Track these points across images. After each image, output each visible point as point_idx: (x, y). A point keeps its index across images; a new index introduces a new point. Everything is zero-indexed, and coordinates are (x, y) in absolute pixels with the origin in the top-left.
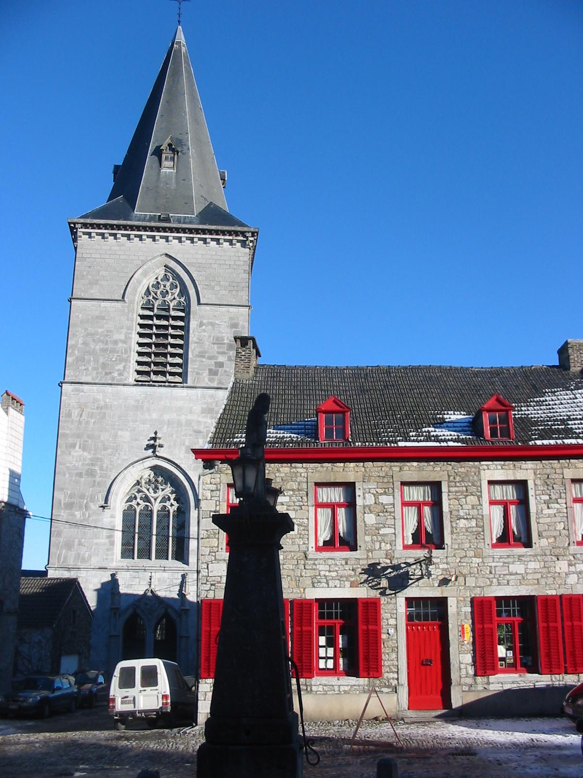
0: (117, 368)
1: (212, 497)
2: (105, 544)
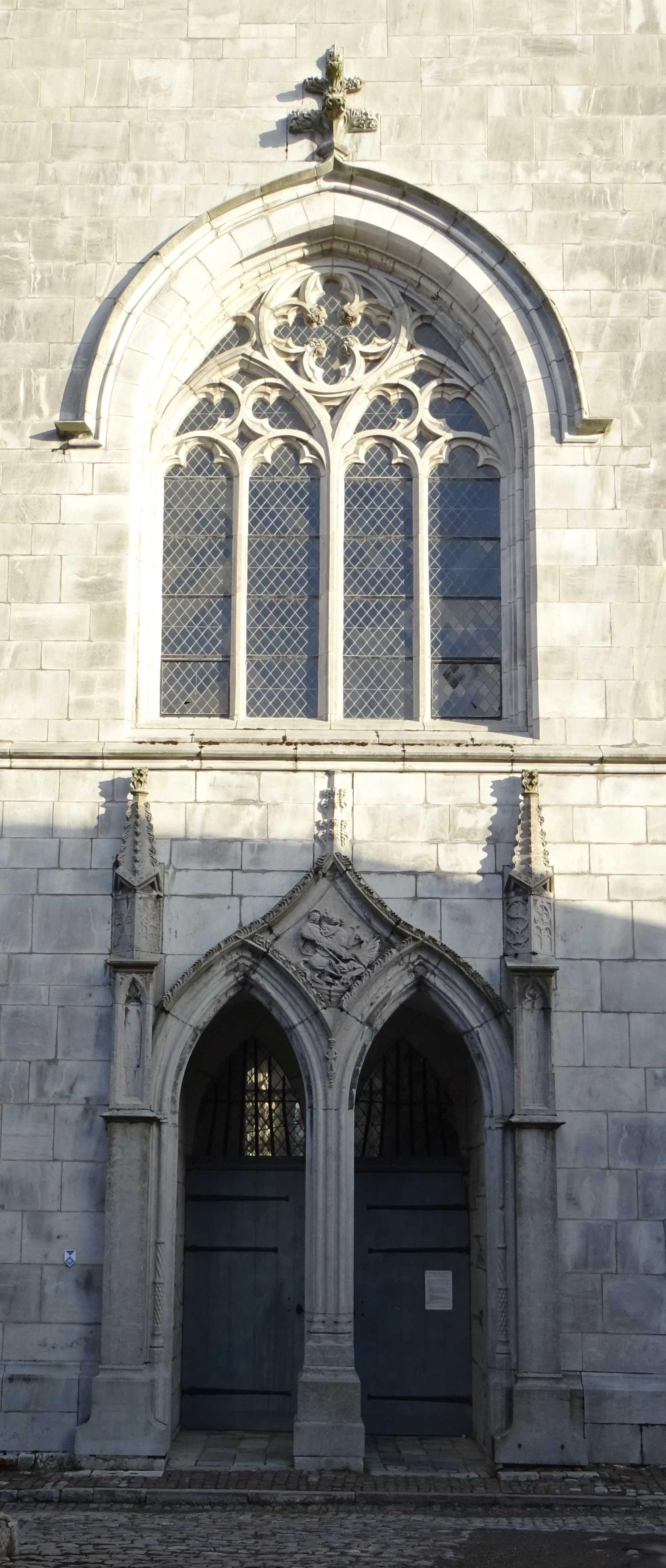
2: (70, 630)
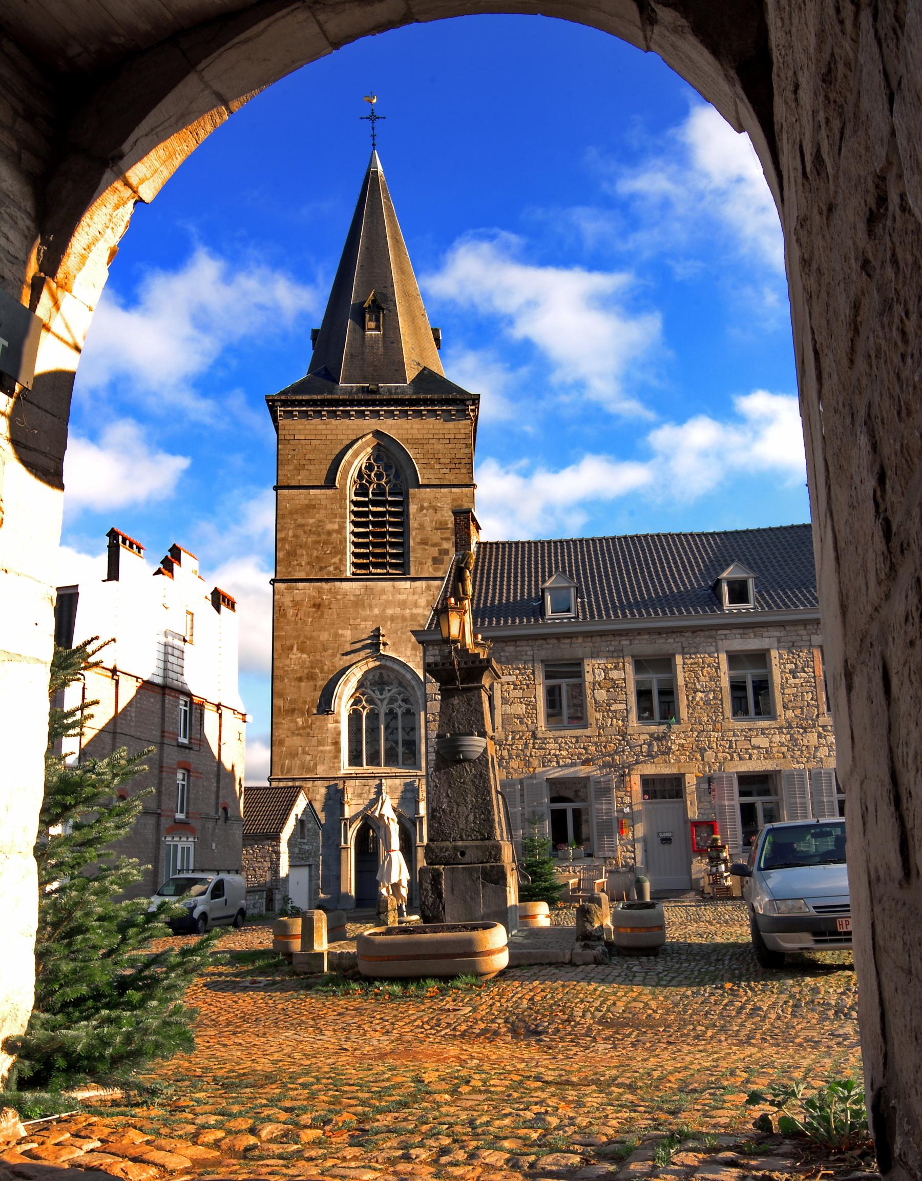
0: (333, 561)
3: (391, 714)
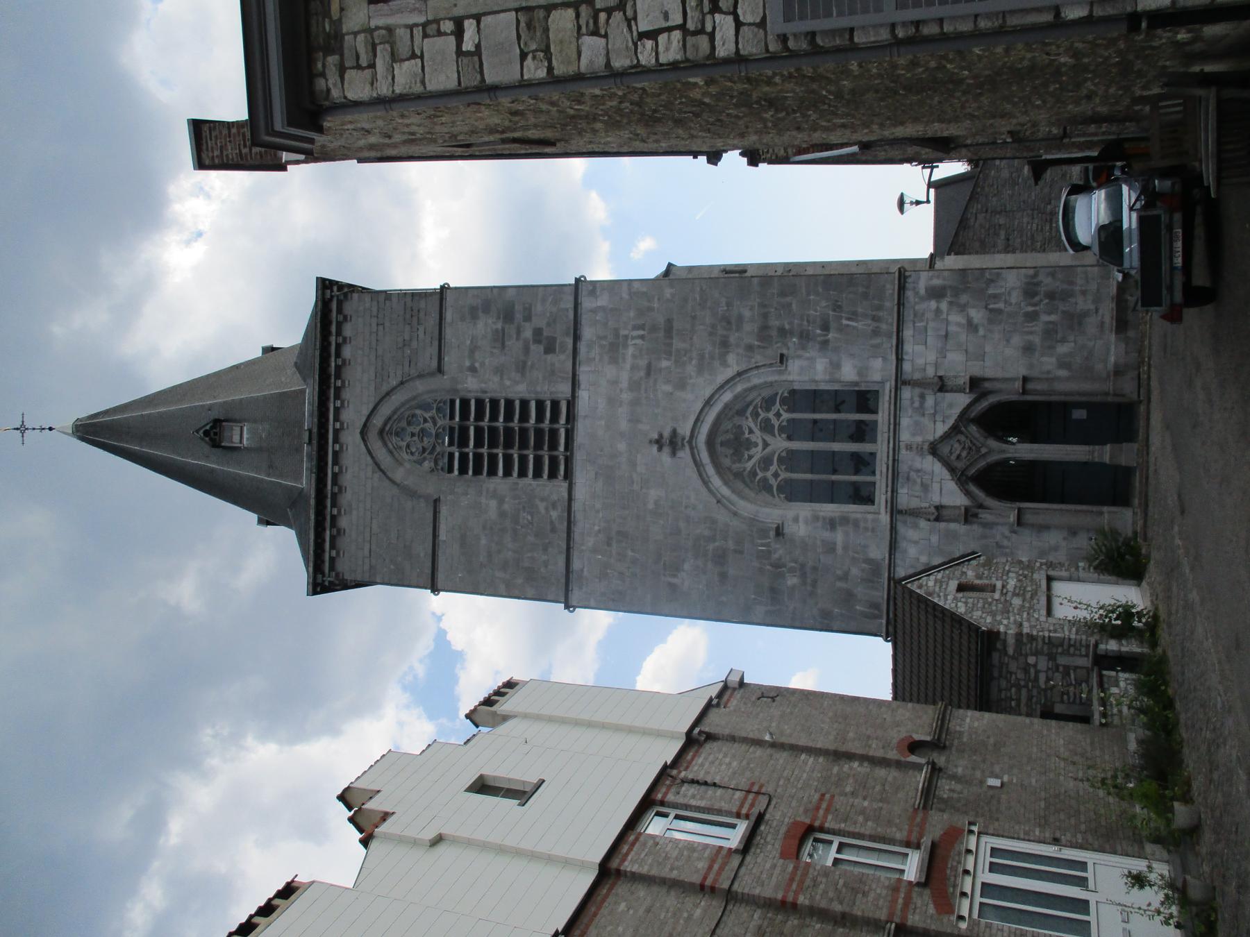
0: (543, 511)
1: (413, 56)
3: (791, 431)
